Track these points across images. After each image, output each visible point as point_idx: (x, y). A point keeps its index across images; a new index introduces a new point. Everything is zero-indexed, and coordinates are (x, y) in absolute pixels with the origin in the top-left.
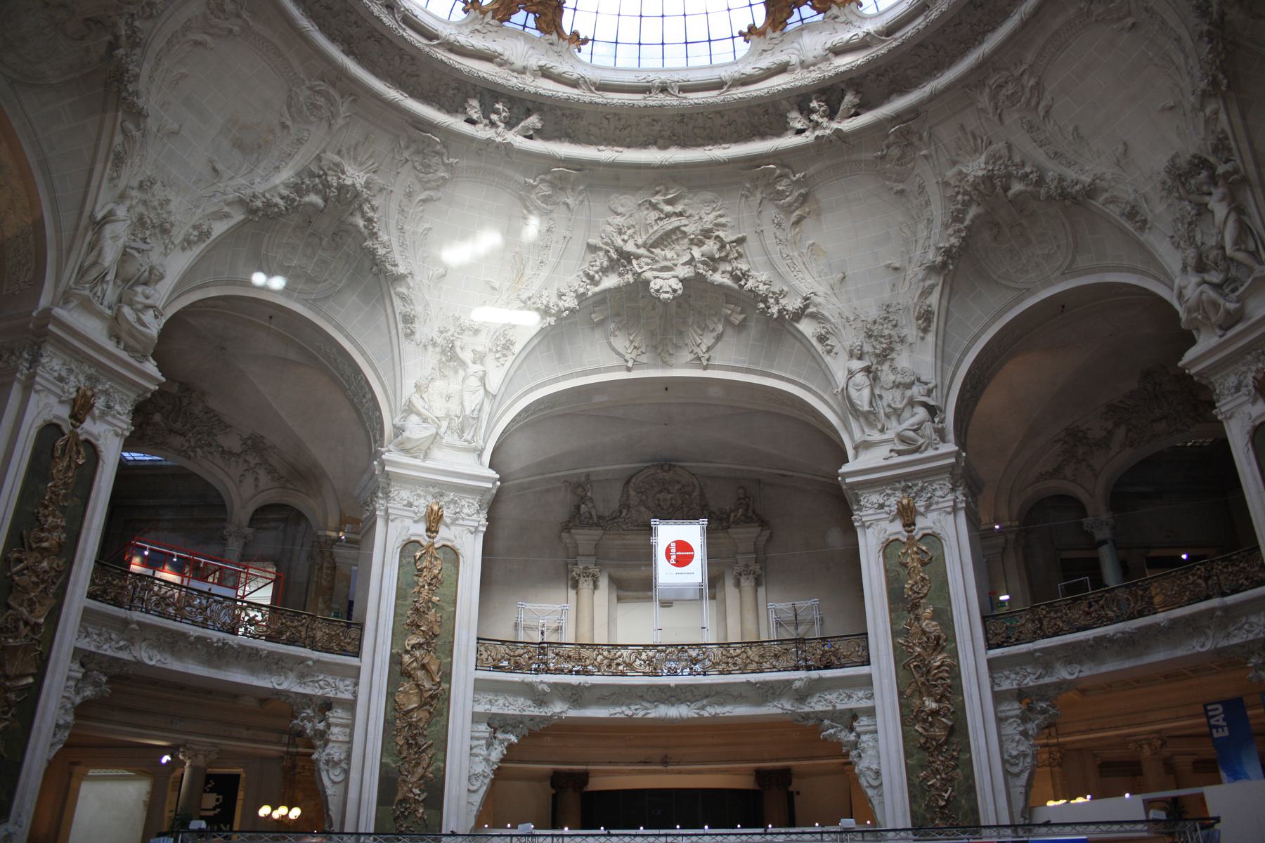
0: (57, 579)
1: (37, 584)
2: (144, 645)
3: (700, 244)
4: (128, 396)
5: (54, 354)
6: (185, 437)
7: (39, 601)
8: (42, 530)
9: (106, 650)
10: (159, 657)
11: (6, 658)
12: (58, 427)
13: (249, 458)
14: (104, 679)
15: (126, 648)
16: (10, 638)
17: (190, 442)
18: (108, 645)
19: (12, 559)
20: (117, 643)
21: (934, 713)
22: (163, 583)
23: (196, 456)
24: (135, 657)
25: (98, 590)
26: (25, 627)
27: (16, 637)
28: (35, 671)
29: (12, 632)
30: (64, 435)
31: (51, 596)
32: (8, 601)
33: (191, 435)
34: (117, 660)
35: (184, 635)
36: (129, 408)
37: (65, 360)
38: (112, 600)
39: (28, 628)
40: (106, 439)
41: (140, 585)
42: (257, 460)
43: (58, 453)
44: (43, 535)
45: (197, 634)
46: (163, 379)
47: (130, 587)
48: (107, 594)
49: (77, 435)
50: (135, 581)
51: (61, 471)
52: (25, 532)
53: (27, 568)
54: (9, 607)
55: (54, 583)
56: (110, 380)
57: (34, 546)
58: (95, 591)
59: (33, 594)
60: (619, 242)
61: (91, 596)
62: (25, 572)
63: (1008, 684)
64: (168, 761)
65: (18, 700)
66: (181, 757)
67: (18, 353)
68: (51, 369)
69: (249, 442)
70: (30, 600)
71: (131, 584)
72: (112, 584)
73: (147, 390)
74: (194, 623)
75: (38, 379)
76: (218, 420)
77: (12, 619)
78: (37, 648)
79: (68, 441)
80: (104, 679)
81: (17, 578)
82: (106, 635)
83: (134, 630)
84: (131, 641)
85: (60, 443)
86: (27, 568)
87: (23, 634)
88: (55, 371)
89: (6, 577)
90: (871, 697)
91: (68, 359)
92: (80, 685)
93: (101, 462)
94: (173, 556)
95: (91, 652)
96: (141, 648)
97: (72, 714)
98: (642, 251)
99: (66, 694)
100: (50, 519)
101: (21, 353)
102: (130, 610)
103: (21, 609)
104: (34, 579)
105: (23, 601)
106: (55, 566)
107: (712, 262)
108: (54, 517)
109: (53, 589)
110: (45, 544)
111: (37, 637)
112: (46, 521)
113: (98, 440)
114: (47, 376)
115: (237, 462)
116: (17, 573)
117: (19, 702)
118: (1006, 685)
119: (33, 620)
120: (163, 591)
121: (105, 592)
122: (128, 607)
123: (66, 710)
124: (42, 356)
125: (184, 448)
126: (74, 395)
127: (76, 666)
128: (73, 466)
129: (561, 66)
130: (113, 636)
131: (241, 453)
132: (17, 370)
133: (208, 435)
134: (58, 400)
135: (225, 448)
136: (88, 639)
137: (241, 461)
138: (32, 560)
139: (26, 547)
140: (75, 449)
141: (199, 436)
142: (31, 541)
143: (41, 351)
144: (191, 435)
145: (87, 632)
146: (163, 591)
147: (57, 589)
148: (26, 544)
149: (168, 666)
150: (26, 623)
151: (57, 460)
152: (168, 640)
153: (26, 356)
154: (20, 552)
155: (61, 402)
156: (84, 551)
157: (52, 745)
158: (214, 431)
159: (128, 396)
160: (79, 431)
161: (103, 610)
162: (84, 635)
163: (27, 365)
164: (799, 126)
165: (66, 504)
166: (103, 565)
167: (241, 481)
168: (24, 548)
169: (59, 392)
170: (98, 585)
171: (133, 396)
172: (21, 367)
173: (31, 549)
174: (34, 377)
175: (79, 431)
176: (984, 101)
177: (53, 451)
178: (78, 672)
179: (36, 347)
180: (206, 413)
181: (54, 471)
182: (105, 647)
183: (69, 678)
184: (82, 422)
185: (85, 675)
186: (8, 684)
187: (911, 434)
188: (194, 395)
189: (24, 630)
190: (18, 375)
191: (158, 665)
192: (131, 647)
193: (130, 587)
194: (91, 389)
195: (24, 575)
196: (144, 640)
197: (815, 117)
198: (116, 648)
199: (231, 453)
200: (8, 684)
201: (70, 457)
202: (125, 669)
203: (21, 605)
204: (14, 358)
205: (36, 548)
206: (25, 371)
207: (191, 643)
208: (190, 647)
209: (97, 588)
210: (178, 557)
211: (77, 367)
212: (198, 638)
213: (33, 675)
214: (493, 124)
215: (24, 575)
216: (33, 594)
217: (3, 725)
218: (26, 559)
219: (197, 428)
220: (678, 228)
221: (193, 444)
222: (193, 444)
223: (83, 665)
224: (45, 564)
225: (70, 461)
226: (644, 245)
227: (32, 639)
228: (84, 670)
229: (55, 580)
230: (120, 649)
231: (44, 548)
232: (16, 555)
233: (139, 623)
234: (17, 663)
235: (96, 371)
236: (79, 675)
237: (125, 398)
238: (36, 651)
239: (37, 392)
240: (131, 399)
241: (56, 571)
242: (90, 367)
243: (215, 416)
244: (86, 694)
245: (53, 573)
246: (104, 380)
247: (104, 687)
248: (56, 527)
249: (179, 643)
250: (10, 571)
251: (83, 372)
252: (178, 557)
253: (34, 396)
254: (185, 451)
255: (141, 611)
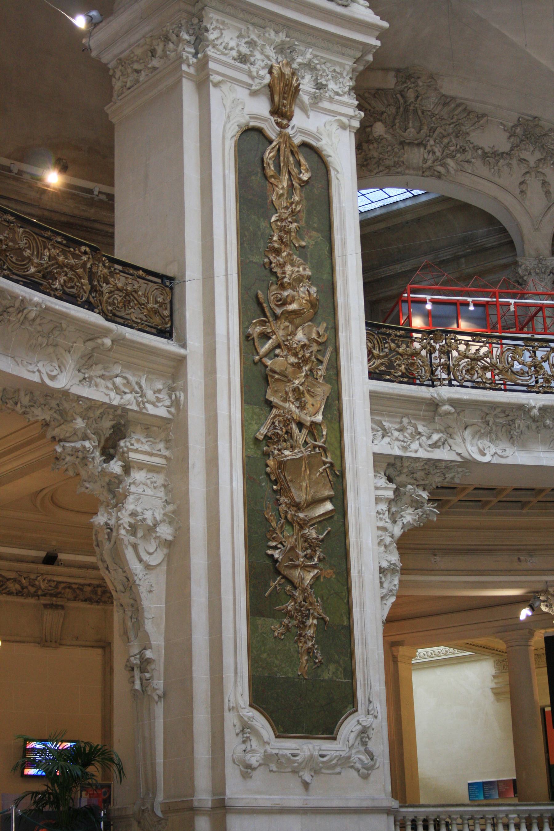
0: (324, 357)
1: (298, 367)
2: (467, 434)
4: (342, 65)
5: (223, 23)
6: (425, 147)
7: (308, 391)
8: (282, 287)
9: (416, 451)
10: (493, 449)
11: (288, 478)
12: (259, 131)
13: (524, 155)
14: (425, 495)
15: (444, 444)
16: (286, 449)
17: (434, 153)
18: (417, 442)
19: (255, 335)
20: (429, 437)
22: (469, 338)
23: (448, 171)
24: (459, 454)
25: (382, 364)
26: (300, 431)
27: (292, 447)
28: (332, 493)
29: (285, 441)
30: (271, 142)
31: (321, 381)
32: (267, 397)
33: (432, 142)
34: (435, 463)
35: (521, 408)
36: (349, 83)
37: (240, 30)
38: (403, 375)
39: (305, 431)
40: (329, 136)
41: (437, 346)
42: (538, 155)
43: (271, 170)
44: (285, 294)
45: (540, 404)
46: (385, 24)
47: (423, 353)
48: (394, 367)
49: (288, 138)
50: (429, 343)
51: (282, 195)
52: (261, 295)
53: (279, 346)
54: (270, 405)
55: (321, 362)
56: (310, 45)
57: (278, 311)
58: (377, 368)
59: (297, 382)
61: (373, 375)
62: (278, 351)
64: (528, 616)
65: (321, 537)
66: (544, 609)
67: (174, 38)
68: (225, 48)
69: (518, 130)
70: (296, 390)
71: (423, 347)
72: (399, 353)
73: (366, 48)
74: (530, 390)
75: (212, 65)
76: (465, 109)
77: (279, 422)
78: (324, 459)
79: (279, 150)
80: (425, 495)
81: (269, 362)
82: (410, 429)
83: (449, 413)
84: (448, 432)
85: (269, 155)
86: (279, 346)
87: (301, 441)
88: (232, 49)
89: (255, 363)
91: (243, 27)
92: (394, 509)
93: (333, 173)
94: (467, 304)
95: (397, 457)
96: (464, 440)
97: (396, 552)
99: (381, 524)
100: (288, 269)
101: (178, 36)
102: (433, 386)
103: (287, 405)
104: (293, 360)
105: (287, 393)
106: (314, 336)
108: (292, 265)
109: (321, 371)
110: (294, 306)
111: (320, 444)
112: (284, 273)
113: (318, 140)
114: (222, 58)
115: (509, 165)
116: (266, 355)
117: (322, 541)
119: (307, 419)
120: (473, 349)
121: (390, 365)
122: (430, 383)
123: (386, 546)
124: (207, 30)
125: (429, 163)
126: (267, 79)
127: (382, 482)
128: (296, 185)
130: (421, 429)
131: (511, 151)
132: (180, 59)
133: (457, 137)
134: (247, 92)
135: (487, 150)
136: (387, 440)
137: (514, 162)
138: (281, 333)
139: (268, 314)
140: (291, 159)
141: (446, 141)
142: (273, 306)
143: (204, 24)
144: (432, 142)
145: (384, 429)
146: (473, 349)
147: (327, 369)
148: (267, 310)
149: (509, 461)
150: (300, 425)
151: (272, 180)
152: (500, 420)
153: (186, 37)
154: (263, 323)
155: (254, 94)
156: (347, 308)
157: (382, 598)
158: (463, 128)
159: (342, 65)
160: (289, 131)
161: (396, 392)
162: (380, 433)
163: (193, 51)
165: (303, 243)
166: (380, 327)
167: (522, 192)
168: (265, 315)
169: (245, 78)
170: (379, 357)
171: (349, 63)
172: (185, 55)
173: (276, 317)
174: (207, 63)
175: (289, 131)
177: (263, 169)
178: (386, 489)
179: (195, 21)
180: (445, 104)
181: (274, 198)
182: (415, 446)
183: (378, 500)
184: (290, 119)
185: (396, 491)
186: (301, 515)
188: (421, 84)
189: (301, 436)
190: (184, 67)
191: (495, 461)
192: (450, 441)
193: (423, 353)
194: (288, 64)
195: (277, 356)
196: (465, 429)
198: (430, 446)
199: (497, 155)
200: (301, 515)
201: (290, 173)
202: (449, 476)
203: (286, 400)
204: (171, 46)
205: (282, 313)
206: (193, 60)
207: (534, 420)
208: (534, 426)
209: (379, 362)
210: (476, 304)
211: (259, 36)
212: (544, 409)
213: (330, 498)
215: (277, 356)
216: (297, 382)
217: (312, 574)
218: (274, 333)
219: (439, 130)
221: (438, 154)
222: (438, 154)
223: (390, 479)
224: (300, 335)
225: (290, 179)
227: (315, 447)
228: (394, 486)
229: (320, 357)
230: (435, 446)
231: (294, 312)
232: (259, 329)
233: (452, 402)
234: (304, 484)
235: (287, 36)
236: (390, 494)
237: (338, 69)
238: (325, 463)
239: (216, 85)
240: (347, 68)
241: (319, 344)
242: (277, 32)
243: (458, 105)
244: (405, 521)
245: (315, 348)
246: (302, 48)
247: (428, 507)
248: (299, 280)
249: (518, 421)
250: (258, 353)
251: (271, 42)
252: (476, 304)
253: (213, 91)
254: (430, 168)
255: (450, 385)
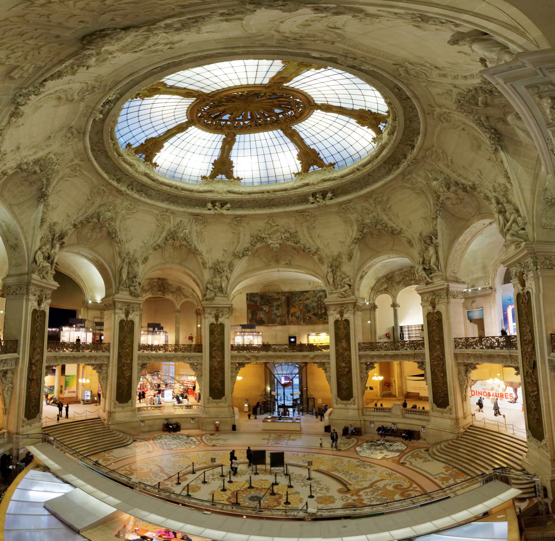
3: (284, 233)
21: (344, 367)
60: (260, 235)
63: (363, 361)
90: (329, 359)
98: (266, 236)
107: (287, 239)
118: (362, 361)
129: (236, 189)
164: (312, 201)
176: (371, 201)
187: (343, 293)
197: (318, 199)
214: (216, 209)
220: (277, 230)
226: (267, 234)
